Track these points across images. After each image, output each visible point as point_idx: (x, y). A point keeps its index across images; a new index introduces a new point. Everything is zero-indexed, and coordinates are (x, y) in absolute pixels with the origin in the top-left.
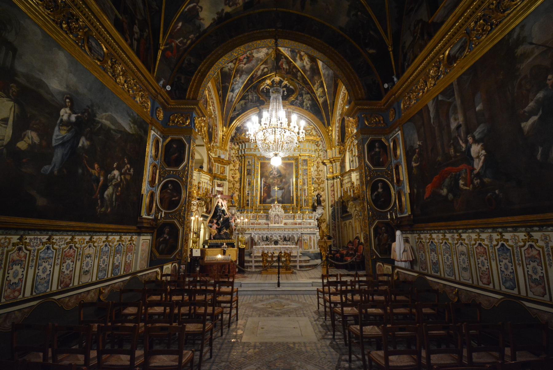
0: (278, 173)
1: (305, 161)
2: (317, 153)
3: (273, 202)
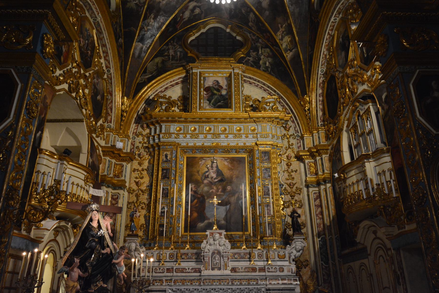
0: (217, 176)
1: (266, 153)
2: (286, 141)
3: (210, 226)
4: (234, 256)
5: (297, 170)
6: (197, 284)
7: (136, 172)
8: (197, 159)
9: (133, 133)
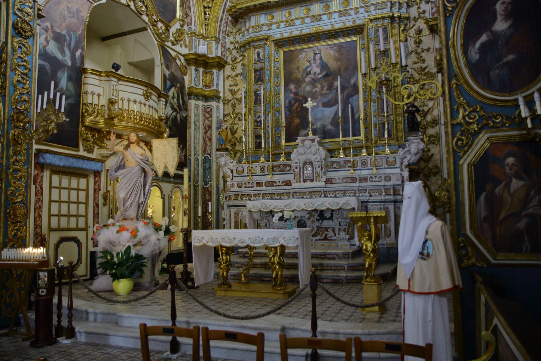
0: (322, 70)
4: (332, 166)
5: (429, 48)
6: (287, 197)
7: (230, 78)
8: (296, 52)
9: (223, 32)
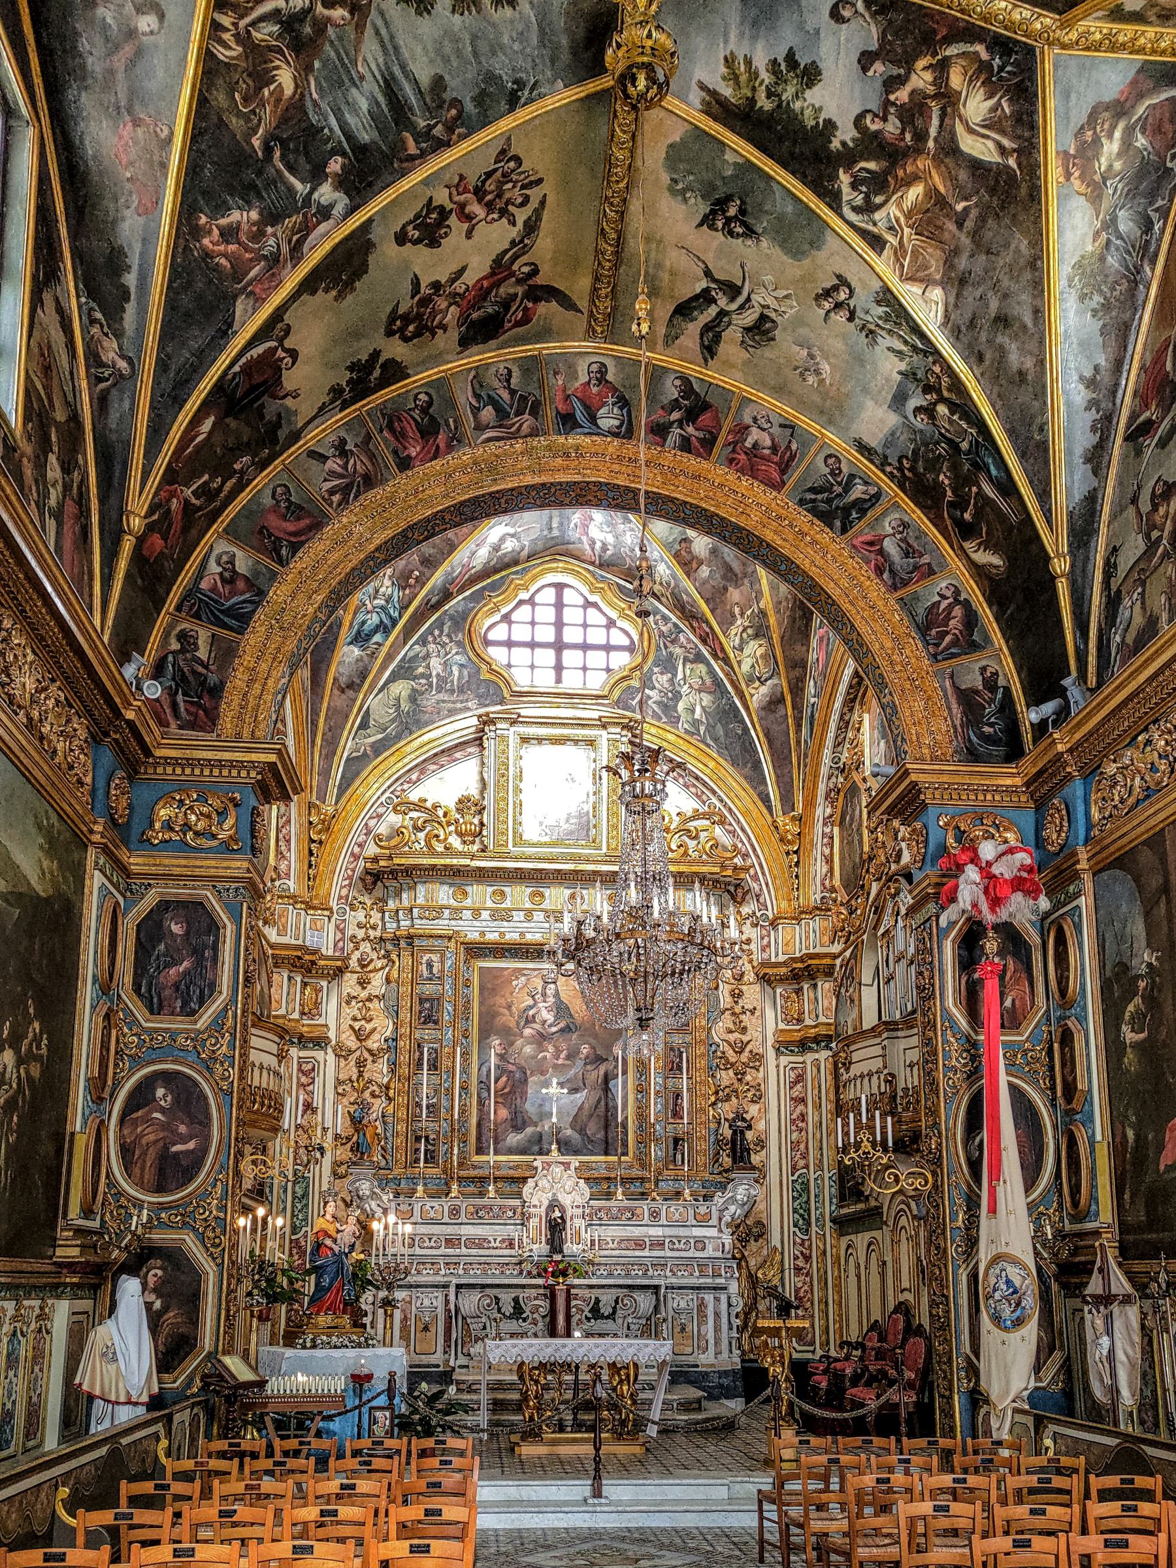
0: (557, 1017)
